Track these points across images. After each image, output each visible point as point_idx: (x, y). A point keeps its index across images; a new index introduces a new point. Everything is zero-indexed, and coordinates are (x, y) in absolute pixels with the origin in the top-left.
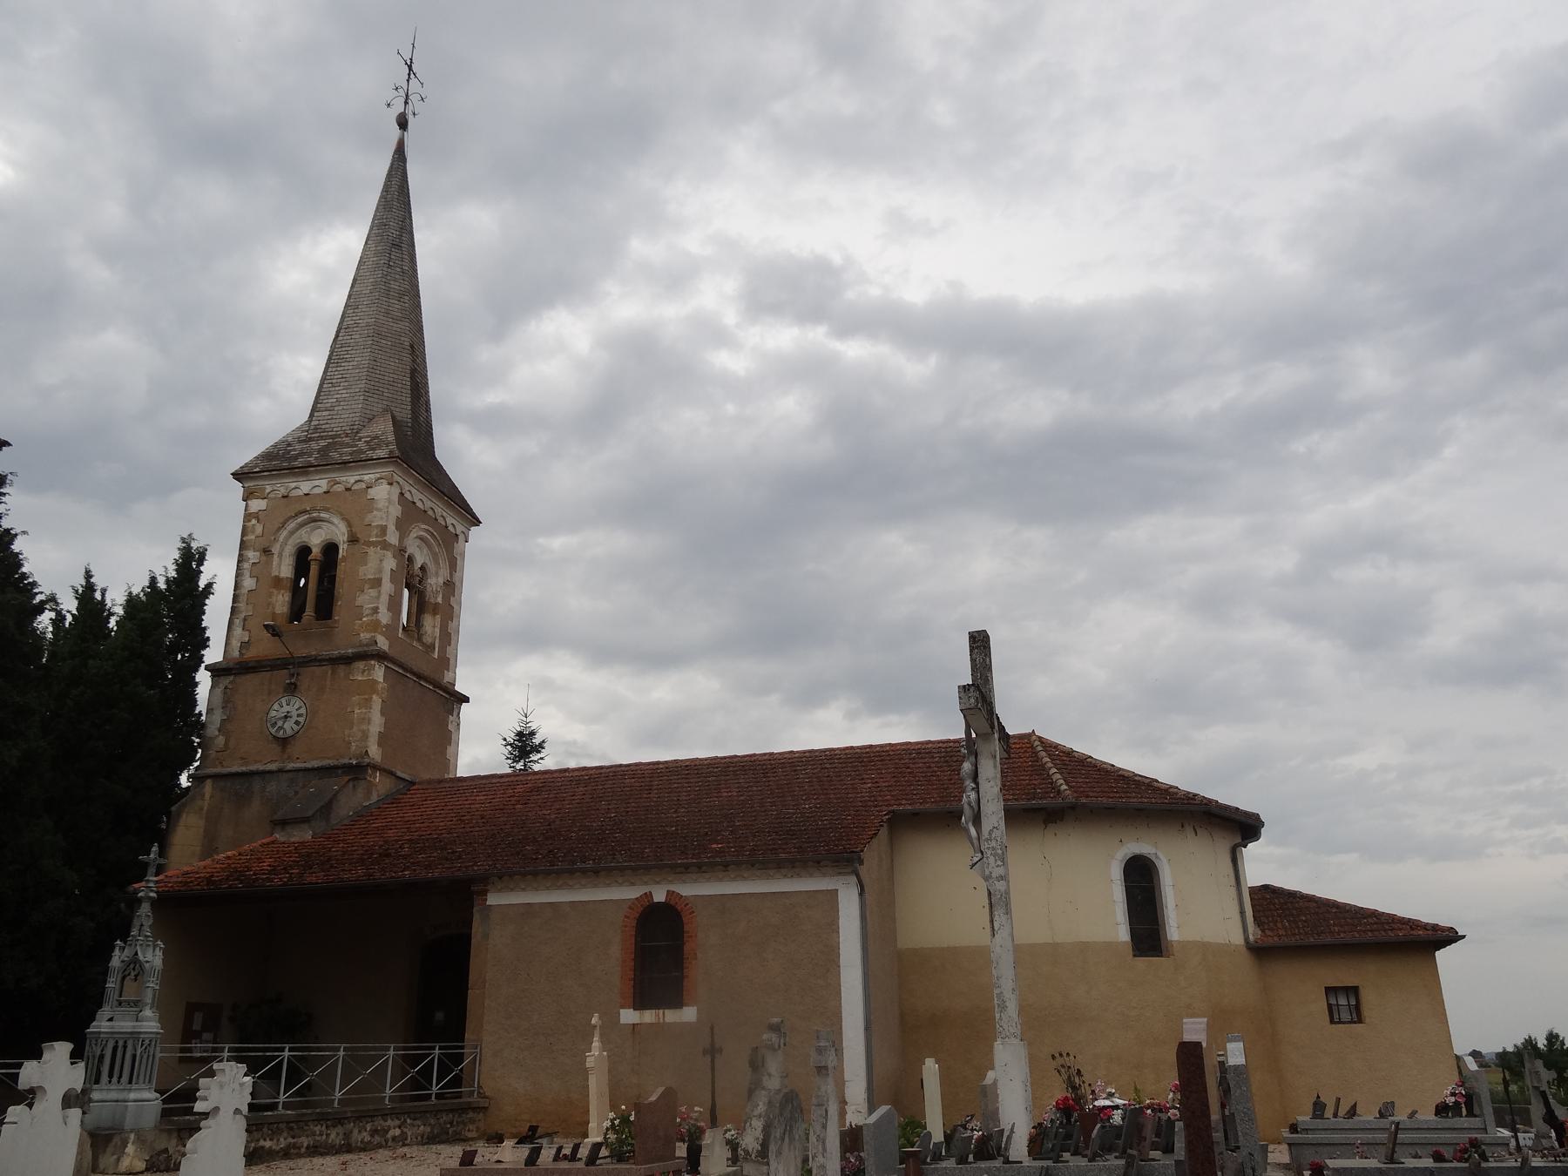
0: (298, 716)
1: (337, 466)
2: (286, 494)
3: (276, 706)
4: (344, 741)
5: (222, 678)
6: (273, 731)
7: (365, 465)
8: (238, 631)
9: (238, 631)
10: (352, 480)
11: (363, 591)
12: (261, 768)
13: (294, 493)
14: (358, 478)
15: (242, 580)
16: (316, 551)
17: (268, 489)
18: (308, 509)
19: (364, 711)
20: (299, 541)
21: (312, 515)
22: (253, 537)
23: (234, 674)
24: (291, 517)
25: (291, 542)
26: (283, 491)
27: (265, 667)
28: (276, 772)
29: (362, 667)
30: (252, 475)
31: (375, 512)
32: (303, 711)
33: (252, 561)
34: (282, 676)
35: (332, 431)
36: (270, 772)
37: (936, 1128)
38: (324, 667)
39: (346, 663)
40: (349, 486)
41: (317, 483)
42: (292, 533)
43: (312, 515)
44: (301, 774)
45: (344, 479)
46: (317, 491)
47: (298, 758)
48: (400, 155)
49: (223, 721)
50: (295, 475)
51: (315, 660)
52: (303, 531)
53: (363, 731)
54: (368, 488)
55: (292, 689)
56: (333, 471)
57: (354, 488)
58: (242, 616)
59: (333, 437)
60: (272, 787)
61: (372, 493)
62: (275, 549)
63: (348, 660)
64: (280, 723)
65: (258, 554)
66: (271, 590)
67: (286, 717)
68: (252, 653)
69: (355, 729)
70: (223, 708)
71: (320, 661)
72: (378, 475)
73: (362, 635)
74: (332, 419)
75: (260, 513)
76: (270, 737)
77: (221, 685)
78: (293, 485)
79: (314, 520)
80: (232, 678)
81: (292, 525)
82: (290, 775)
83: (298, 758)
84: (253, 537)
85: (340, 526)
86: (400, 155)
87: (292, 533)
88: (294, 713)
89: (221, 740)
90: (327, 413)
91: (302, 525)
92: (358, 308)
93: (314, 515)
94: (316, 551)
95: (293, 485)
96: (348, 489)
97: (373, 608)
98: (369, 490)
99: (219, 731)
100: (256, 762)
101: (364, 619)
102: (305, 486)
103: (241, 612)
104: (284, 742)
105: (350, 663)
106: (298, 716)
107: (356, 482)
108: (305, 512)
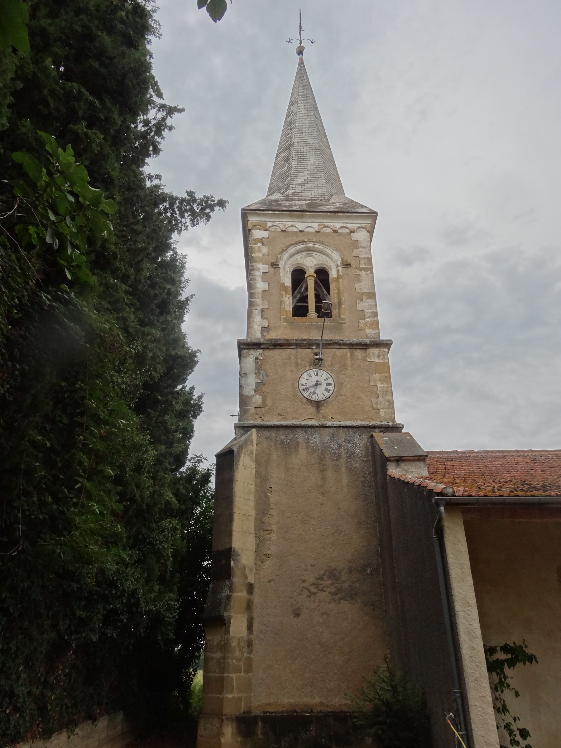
0: (327, 384)
1: (329, 214)
2: (284, 229)
3: (305, 376)
4: (372, 407)
5: (252, 350)
6: (306, 394)
7: (350, 216)
8: (257, 318)
9: (257, 318)
10: (338, 226)
11: (362, 300)
12: (303, 423)
13: (290, 230)
14: (343, 225)
15: (255, 283)
16: (310, 272)
17: (269, 224)
18: (306, 240)
19: (386, 385)
20: (296, 263)
21: (307, 245)
22: (260, 255)
23: (263, 349)
24: (293, 244)
25: (289, 262)
26: (282, 227)
27: (290, 345)
28: (318, 427)
29: (377, 352)
30: (258, 212)
31: (360, 249)
32: (331, 381)
33: (262, 271)
34: (307, 353)
35: (308, 197)
36: (312, 427)
37: (459, 691)
38: (344, 350)
39: (363, 349)
40: (336, 229)
41: (309, 224)
42: (291, 256)
43: (307, 245)
44: (341, 430)
45: (332, 224)
46: (309, 230)
47: (332, 418)
48: (301, 62)
49: (257, 384)
50: (291, 216)
51: (337, 343)
52: (298, 257)
53: (388, 401)
54: (351, 232)
55: (318, 363)
56: (323, 217)
57: (340, 231)
58: (260, 308)
59: (312, 200)
60: (316, 438)
61: (355, 236)
62: (281, 264)
63: (364, 346)
64: (312, 390)
65: (267, 266)
66: (282, 292)
67: (317, 385)
68: (273, 335)
69: (380, 399)
70: (256, 373)
71: (340, 344)
72: (359, 225)
73: (367, 330)
74: (305, 190)
75: (263, 239)
76: (304, 400)
77: (251, 356)
78: (290, 224)
79: (308, 250)
80: (261, 351)
81: (292, 250)
82: (331, 430)
83: (332, 418)
84: (260, 255)
85: (333, 255)
86: (301, 62)
87: (291, 256)
88: (324, 383)
89: (258, 399)
90: (300, 187)
91: (298, 252)
92: (302, 134)
93: (310, 245)
94: (310, 272)
95: (290, 224)
96: (335, 232)
97: (372, 313)
98: (352, 234)
99: (255, 391)
100: (293, 418)
101: (367, 320)
102: (300, 225)
103: (258, 305)
104: (318, 404)
105: (366, 349)
106: (327, 384)
107: (342, 227)
108: (303, 242)
